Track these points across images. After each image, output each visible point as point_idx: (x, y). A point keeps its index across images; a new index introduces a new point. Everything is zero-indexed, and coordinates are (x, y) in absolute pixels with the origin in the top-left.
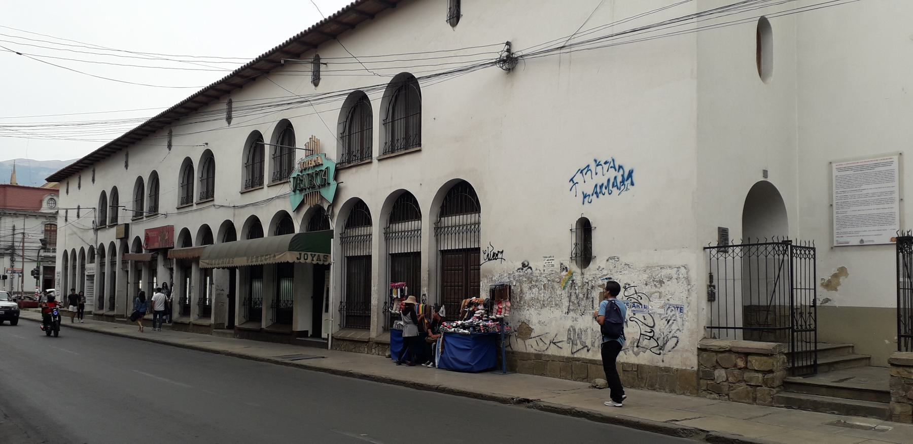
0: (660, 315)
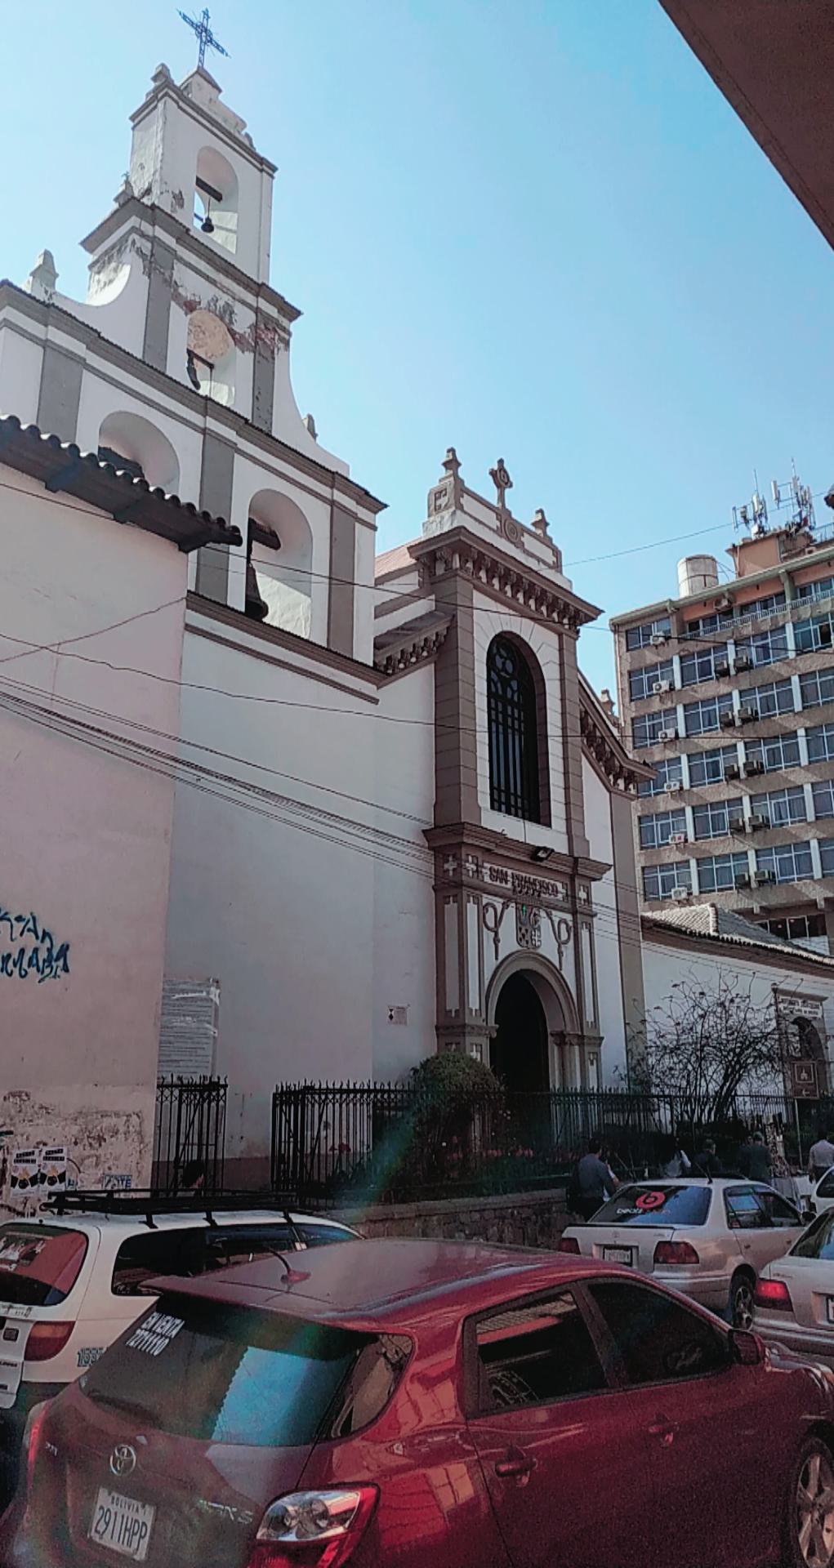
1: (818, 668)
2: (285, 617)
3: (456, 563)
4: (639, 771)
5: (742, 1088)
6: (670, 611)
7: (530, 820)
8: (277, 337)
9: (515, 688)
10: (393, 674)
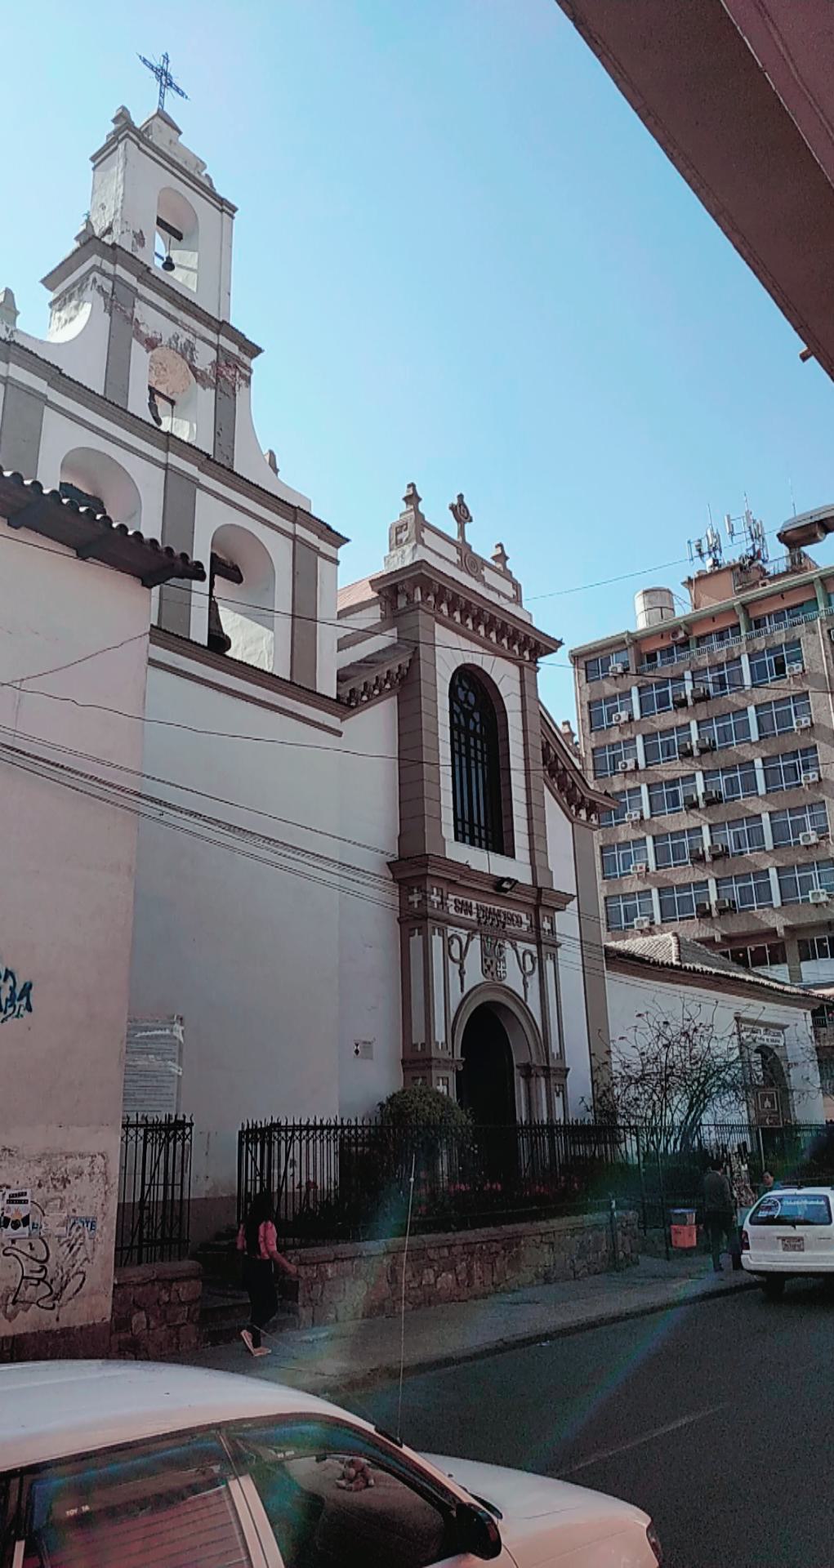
0: (59, 1237)
1: (774, 698)
2: (248, 650)
3: (418, 597)
4: (601, 802)
5: (707, 1118)
6: (628, 643)
7: (493, 851)
8: (238, 374)
9: (478, 720)
10: (356, 707)
